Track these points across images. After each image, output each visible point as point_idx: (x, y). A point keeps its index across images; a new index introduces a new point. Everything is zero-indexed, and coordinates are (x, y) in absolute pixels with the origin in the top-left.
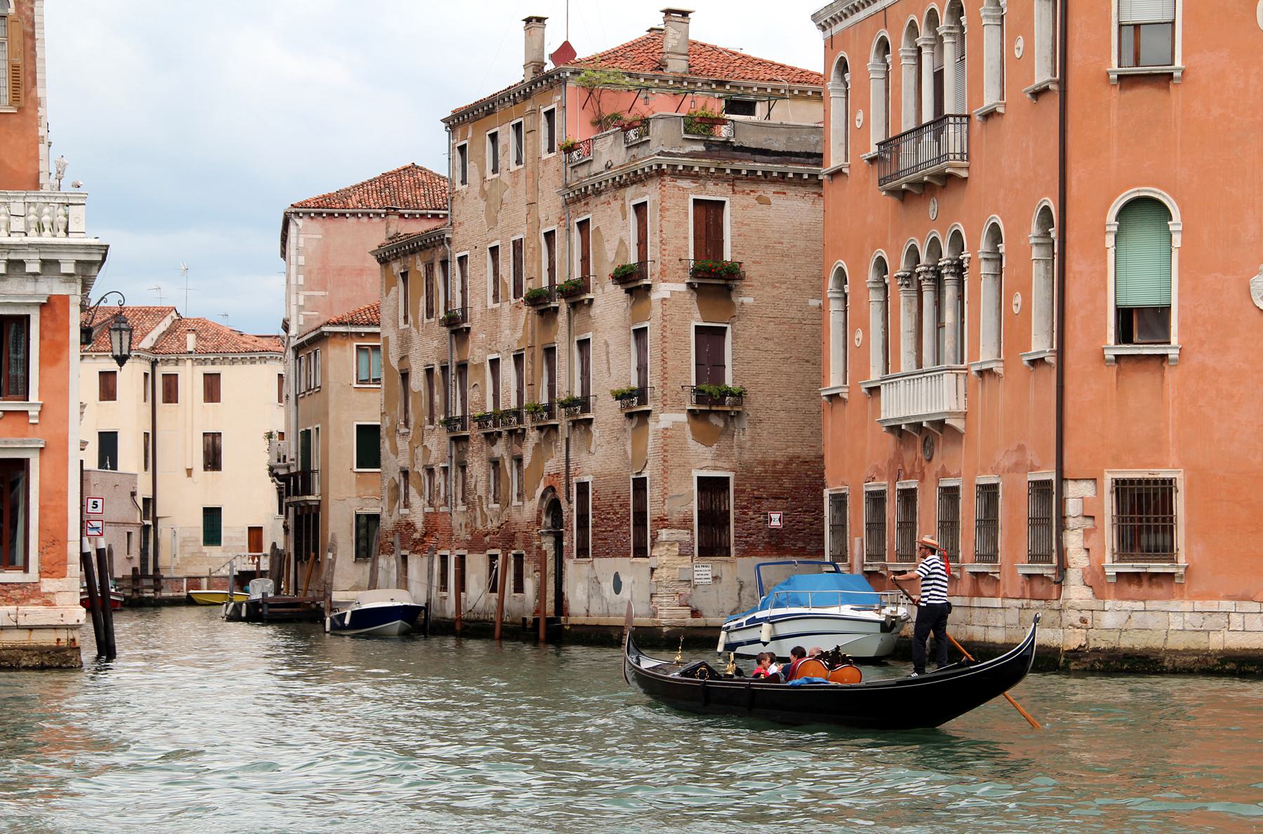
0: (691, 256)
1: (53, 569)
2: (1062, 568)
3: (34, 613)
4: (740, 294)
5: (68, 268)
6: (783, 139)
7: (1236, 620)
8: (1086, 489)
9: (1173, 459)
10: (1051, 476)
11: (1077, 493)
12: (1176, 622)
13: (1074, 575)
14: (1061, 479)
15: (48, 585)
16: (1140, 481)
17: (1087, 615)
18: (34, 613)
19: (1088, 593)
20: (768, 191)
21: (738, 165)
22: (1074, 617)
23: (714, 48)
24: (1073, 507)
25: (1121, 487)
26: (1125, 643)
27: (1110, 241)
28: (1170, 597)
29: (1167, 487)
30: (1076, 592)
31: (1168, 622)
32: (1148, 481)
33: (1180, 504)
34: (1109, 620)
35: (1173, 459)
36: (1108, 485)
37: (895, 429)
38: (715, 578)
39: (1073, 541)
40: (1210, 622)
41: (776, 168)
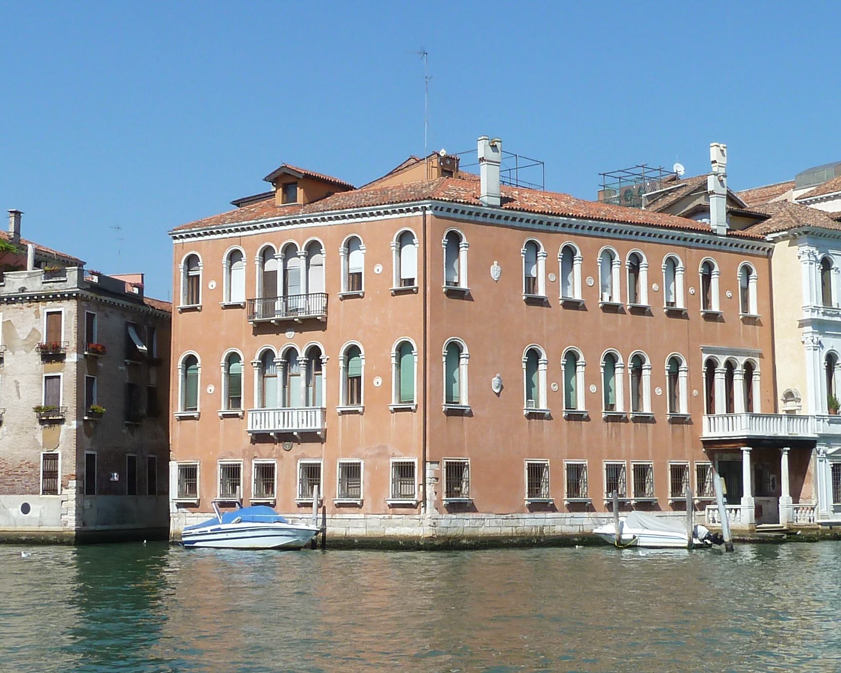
9: (466, 454)
10: (416, 461)
12: (467, 523)
31: (463, 525)
34: (443, 523)
35: (466, 454)
39: (430, 489)
40: (478, 523)
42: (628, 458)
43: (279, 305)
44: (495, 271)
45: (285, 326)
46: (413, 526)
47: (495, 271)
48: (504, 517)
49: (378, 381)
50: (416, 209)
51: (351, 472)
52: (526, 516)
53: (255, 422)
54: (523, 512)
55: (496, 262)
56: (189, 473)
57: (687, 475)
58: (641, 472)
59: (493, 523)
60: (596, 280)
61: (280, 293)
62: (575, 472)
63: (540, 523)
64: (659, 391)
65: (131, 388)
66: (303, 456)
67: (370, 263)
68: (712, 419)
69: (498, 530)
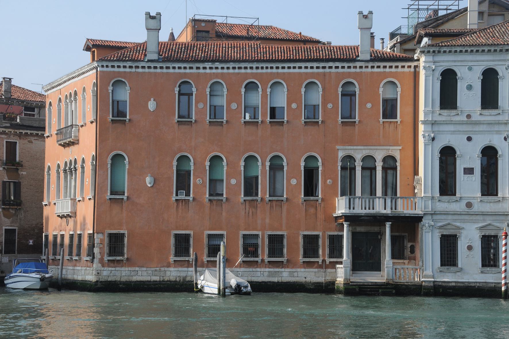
0: (5, 159)
2: (94, 258)
4: (22, 171)
6: (37, 123)
7: (140, 273)
8: (100, 236)
9: (125, 227)
13: (96, 261)
16: (115, 234)
17: (99, 272)
19: (100, 265)
20: (32, 139)
21: (21, 131)
23: (23, 89)
24: (96, 241)
25: (111, 236)
26: (110, 279)
27: (109, 166)
28: (122, 267)
29: (123, 235)
32: (117, 234)
33: (126, 240)
34: (105, 273)
36: (106, 235)
37: (59, 216)
38: (9, 261)
41: (35, 132)
42: (263, 229)
44: (152, 105)
47: (152, 105)
48: (154, 269)
52: (172, 269)
54: (169, 266)
55: (152, 99)
60: (239, 105)
63: (183, 274)
68: (352, 200)
69: (148, 278)
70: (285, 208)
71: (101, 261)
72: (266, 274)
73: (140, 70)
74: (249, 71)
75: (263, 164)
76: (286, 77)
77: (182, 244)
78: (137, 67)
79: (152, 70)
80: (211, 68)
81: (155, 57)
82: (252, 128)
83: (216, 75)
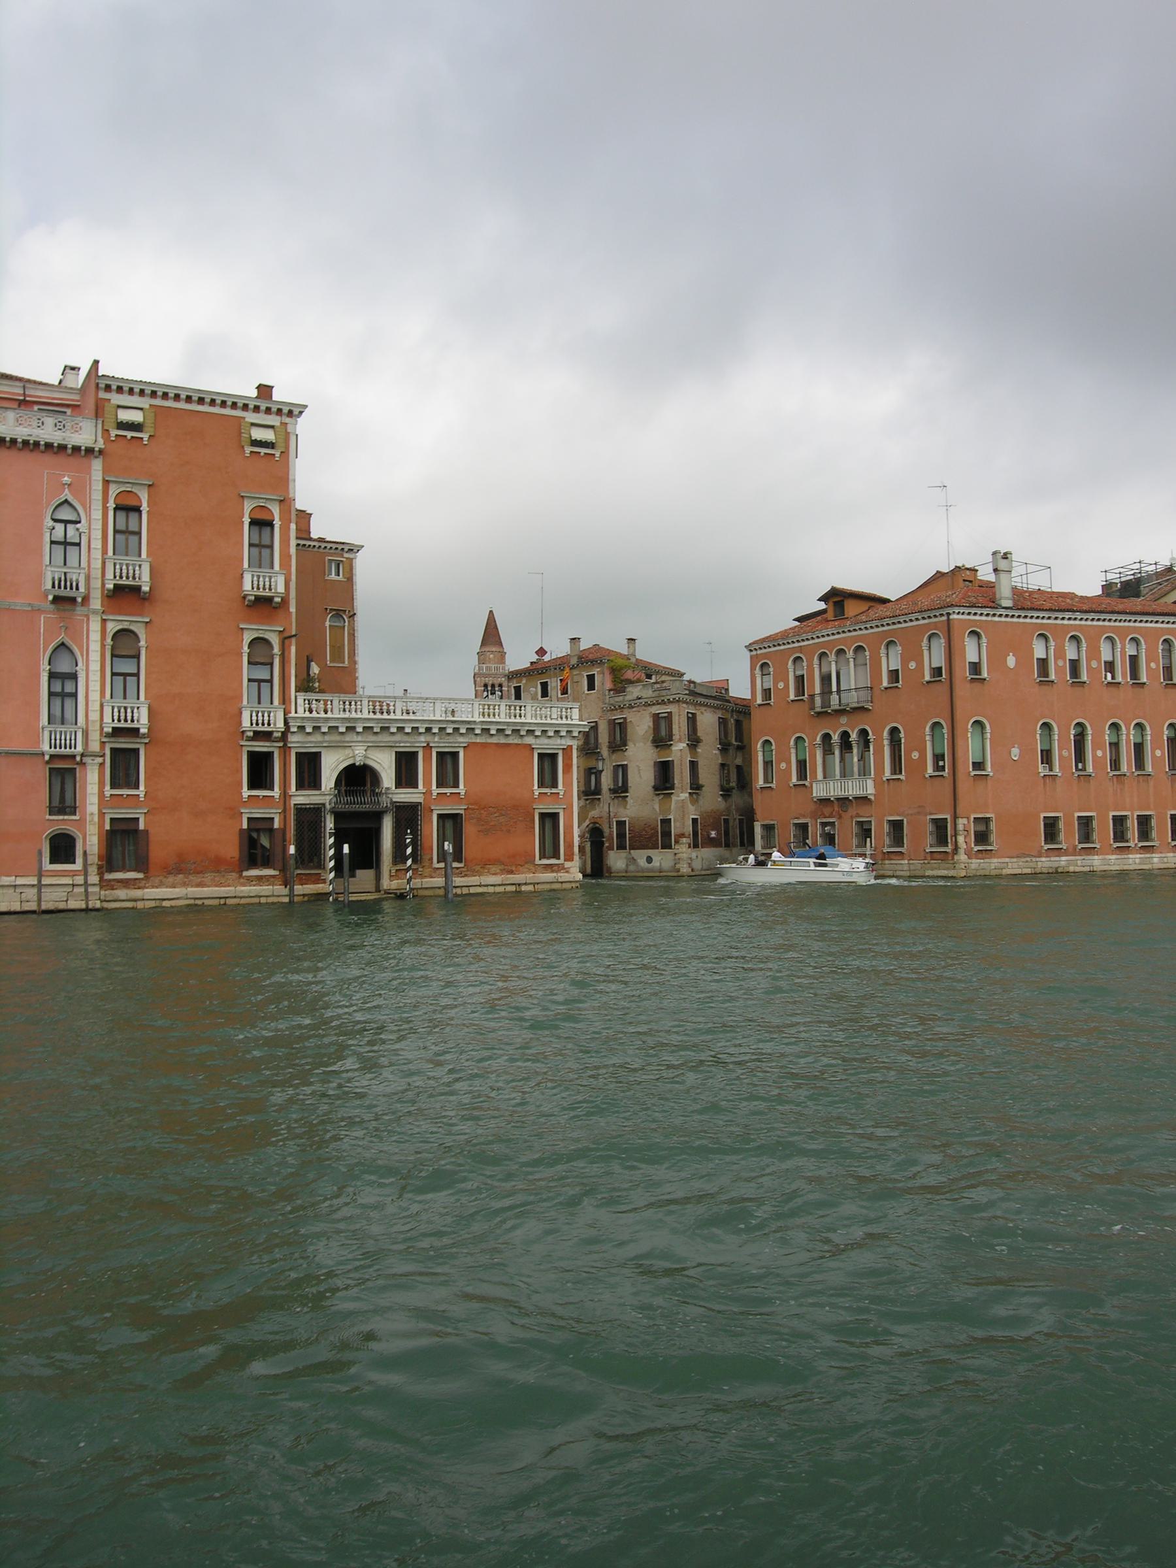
1: (569, 858)
3: (563, 876)
5: (575, 734)
8: (965, 821)
11: (961, 822)
13: (962, 851)
14: (955, 817)
15: (568, 864)
18: (563, 876)
22: (963, 866)
24: (960, 827)
30: (962, 857)
34: (973, 866)
39: (961, 839)
43: (834, 699)
44: (1011, 661)
45: (840, 712)
46: (948, 869)
47: (1011, 661)
49: (915, 755)
50: (942, 615)
51: (897, 826)
53: (819, 790)
56: (769, 829)
57: (1129, 823)
58: (1144, 821)
59: (1015, 865)
61: (834, 688)
62: (1085, 823)
63: (1055, 865)
64: (1158, 753)
65: (723, 765)
66: (858, 816)
67: (905, 661)
70: (1151, 783)
71: (969, 854)
72: (1137, 861)
73: (996, 619)
74: (1106, 623)
75: (1128, 735)
76: (1145, 632)
77: (1051, 828)
78: (994, 615)
79: (1009, 619)
80: (1069, 619)
81: (1009, 603)
82: (1112, 689)
83: (1075, 627)
